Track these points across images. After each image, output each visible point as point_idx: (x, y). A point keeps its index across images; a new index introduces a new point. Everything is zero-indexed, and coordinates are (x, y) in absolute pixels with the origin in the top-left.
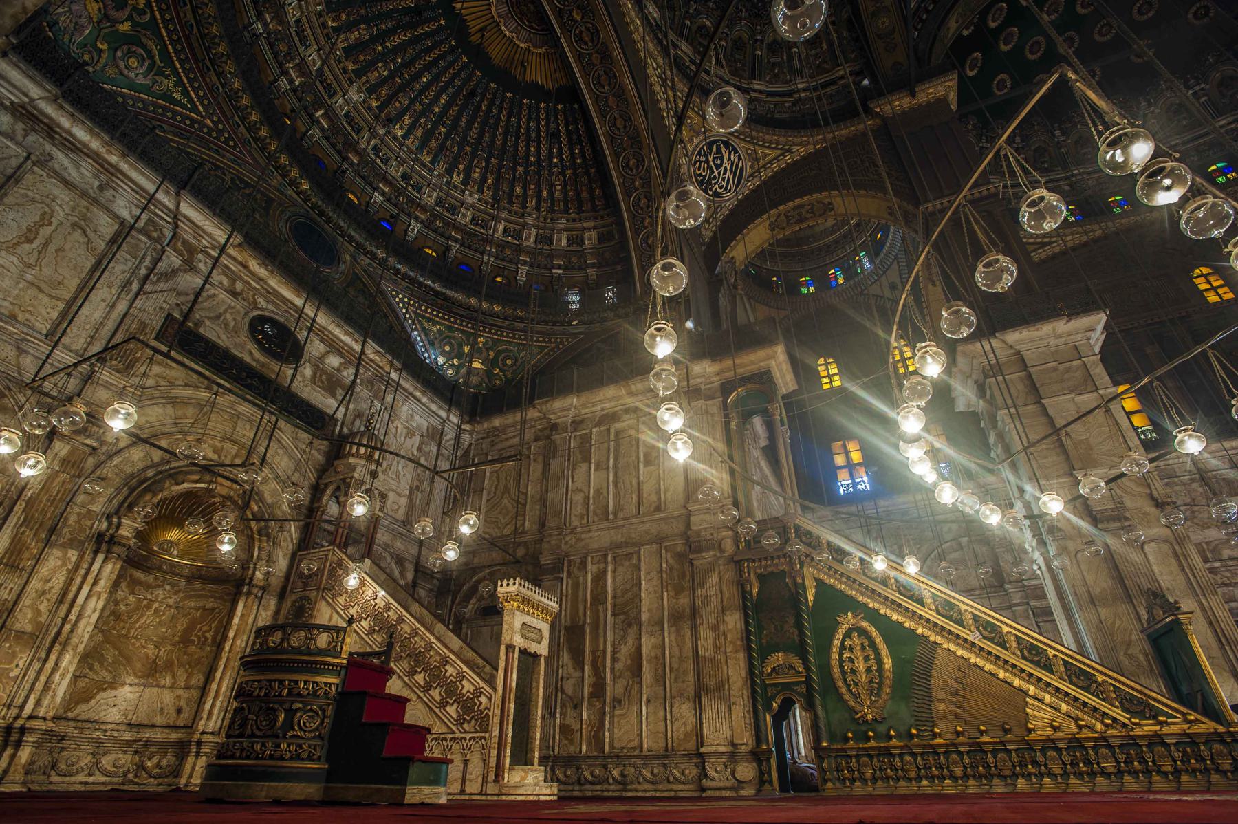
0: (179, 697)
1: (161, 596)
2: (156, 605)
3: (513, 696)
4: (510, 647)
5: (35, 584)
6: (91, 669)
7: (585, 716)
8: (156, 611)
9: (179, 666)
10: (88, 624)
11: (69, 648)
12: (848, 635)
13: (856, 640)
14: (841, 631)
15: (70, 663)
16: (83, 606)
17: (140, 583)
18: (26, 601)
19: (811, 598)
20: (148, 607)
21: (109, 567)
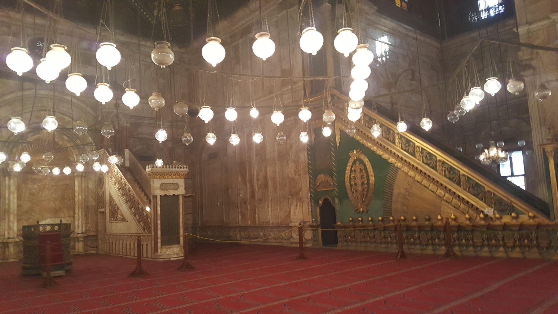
2: (47, 187)
3: (159, 218)
4: (155, 197)
12: (354, 163)
13: (358, 166)
14: (351, 161)
19: (338, 142)
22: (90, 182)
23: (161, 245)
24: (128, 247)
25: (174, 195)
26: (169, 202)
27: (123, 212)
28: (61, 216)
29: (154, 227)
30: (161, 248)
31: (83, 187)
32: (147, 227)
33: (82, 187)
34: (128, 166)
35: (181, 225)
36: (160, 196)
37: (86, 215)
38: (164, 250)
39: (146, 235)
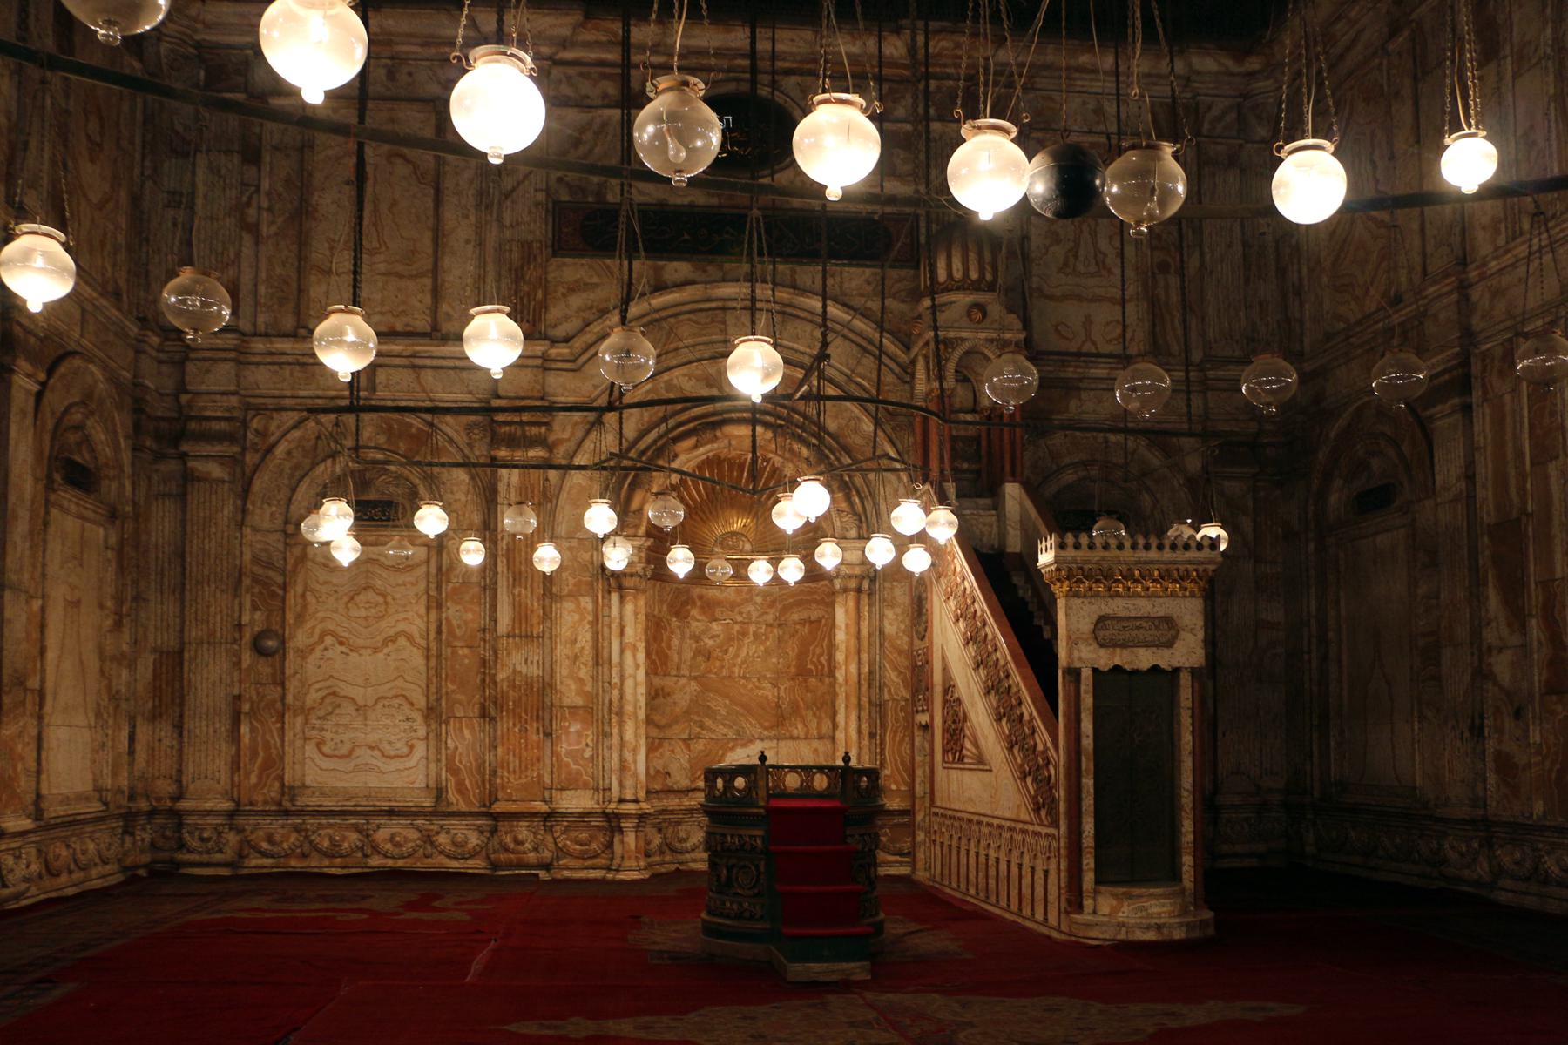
0: (816, 750)
1: (754, 616)
2: (752, 628)
3: (1087, 764)
4: (1074, 674)
5: (561, 651)
6: (702, 727)
7: (1535, 736)
8: (756, 635)
9: (807, 708)
10: (636, 684)
11: (626, 718)
15: (636, 735)
16: (621, 664)
17: (719, 603)
18: (562, 671)
20: (744, 634)
21: (629, 607)
22: (889, 614)
23: (1098, 882)
24: (992, 872)
25: (1155, 669)
26: (1130, 699)
27: (979, 732)
28: (795, 732)
29: (1068, 801)
30: (1096, 892)
31: (865, 632)
32: (1043, 803)
33: (859, 632)
34: (1018, 550)
35: (1187, 800)
36: (1095, 670)
37: (872, 735)
38: (1106, 904)
39: (1044, 830)
